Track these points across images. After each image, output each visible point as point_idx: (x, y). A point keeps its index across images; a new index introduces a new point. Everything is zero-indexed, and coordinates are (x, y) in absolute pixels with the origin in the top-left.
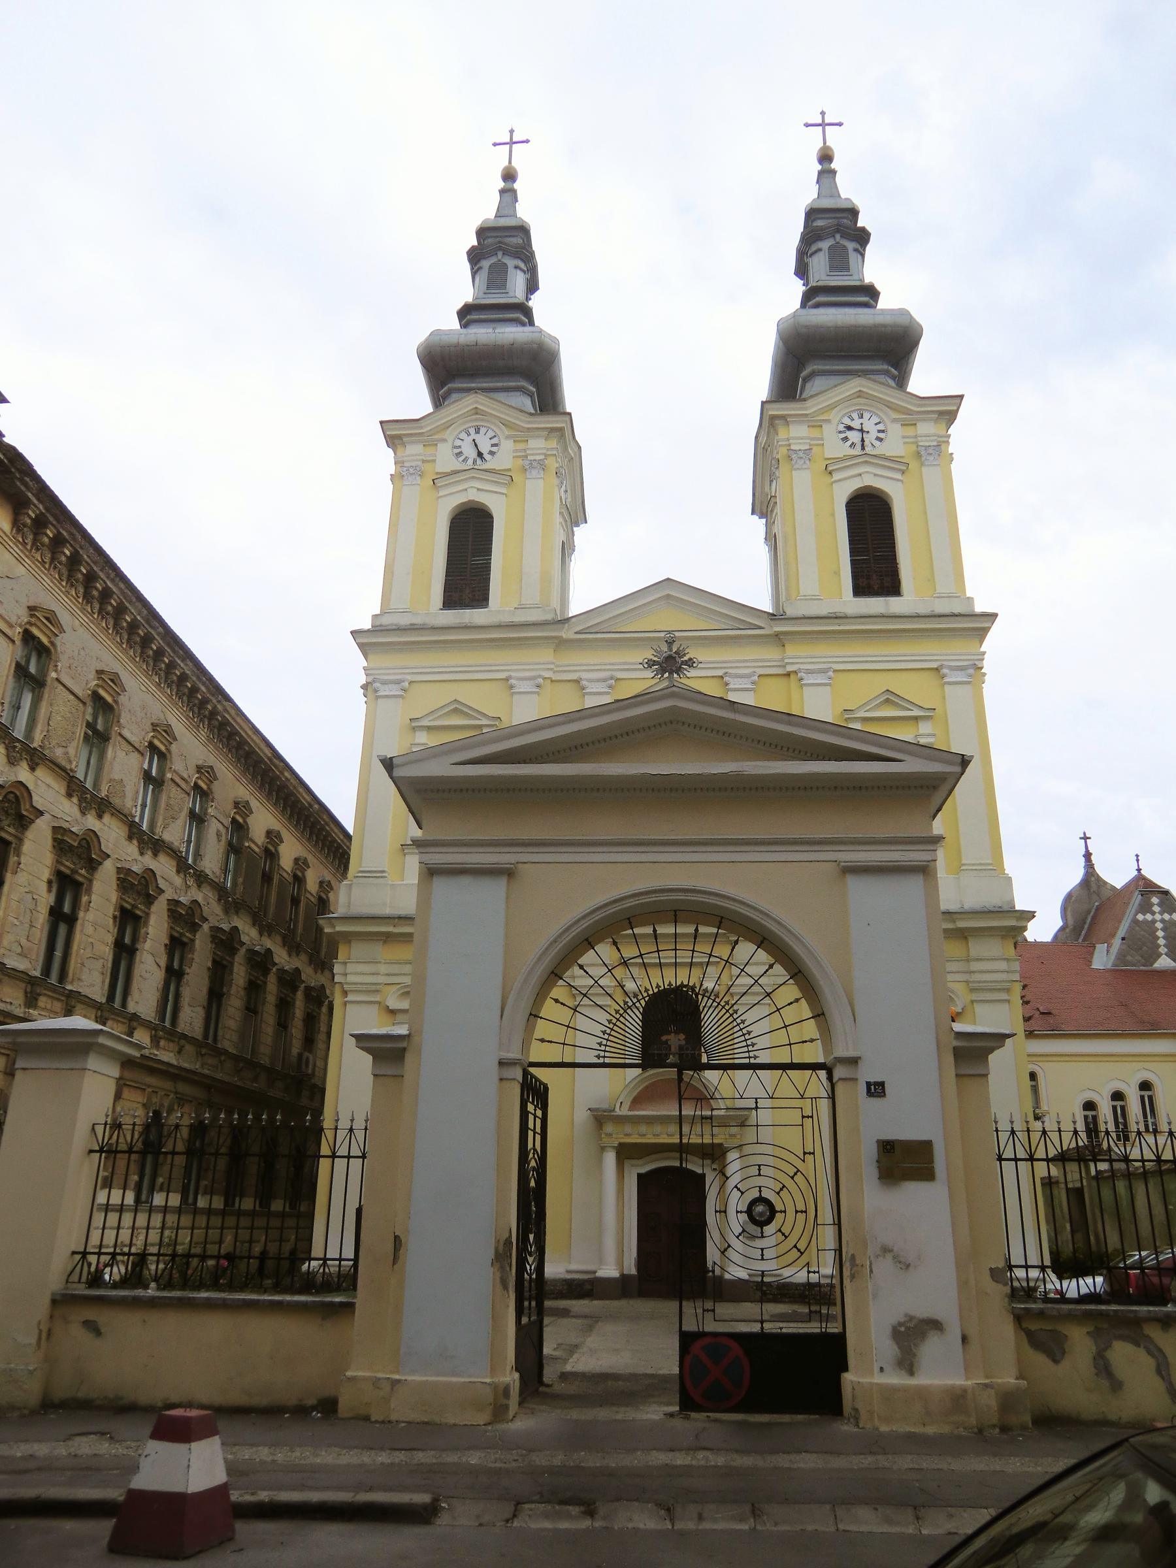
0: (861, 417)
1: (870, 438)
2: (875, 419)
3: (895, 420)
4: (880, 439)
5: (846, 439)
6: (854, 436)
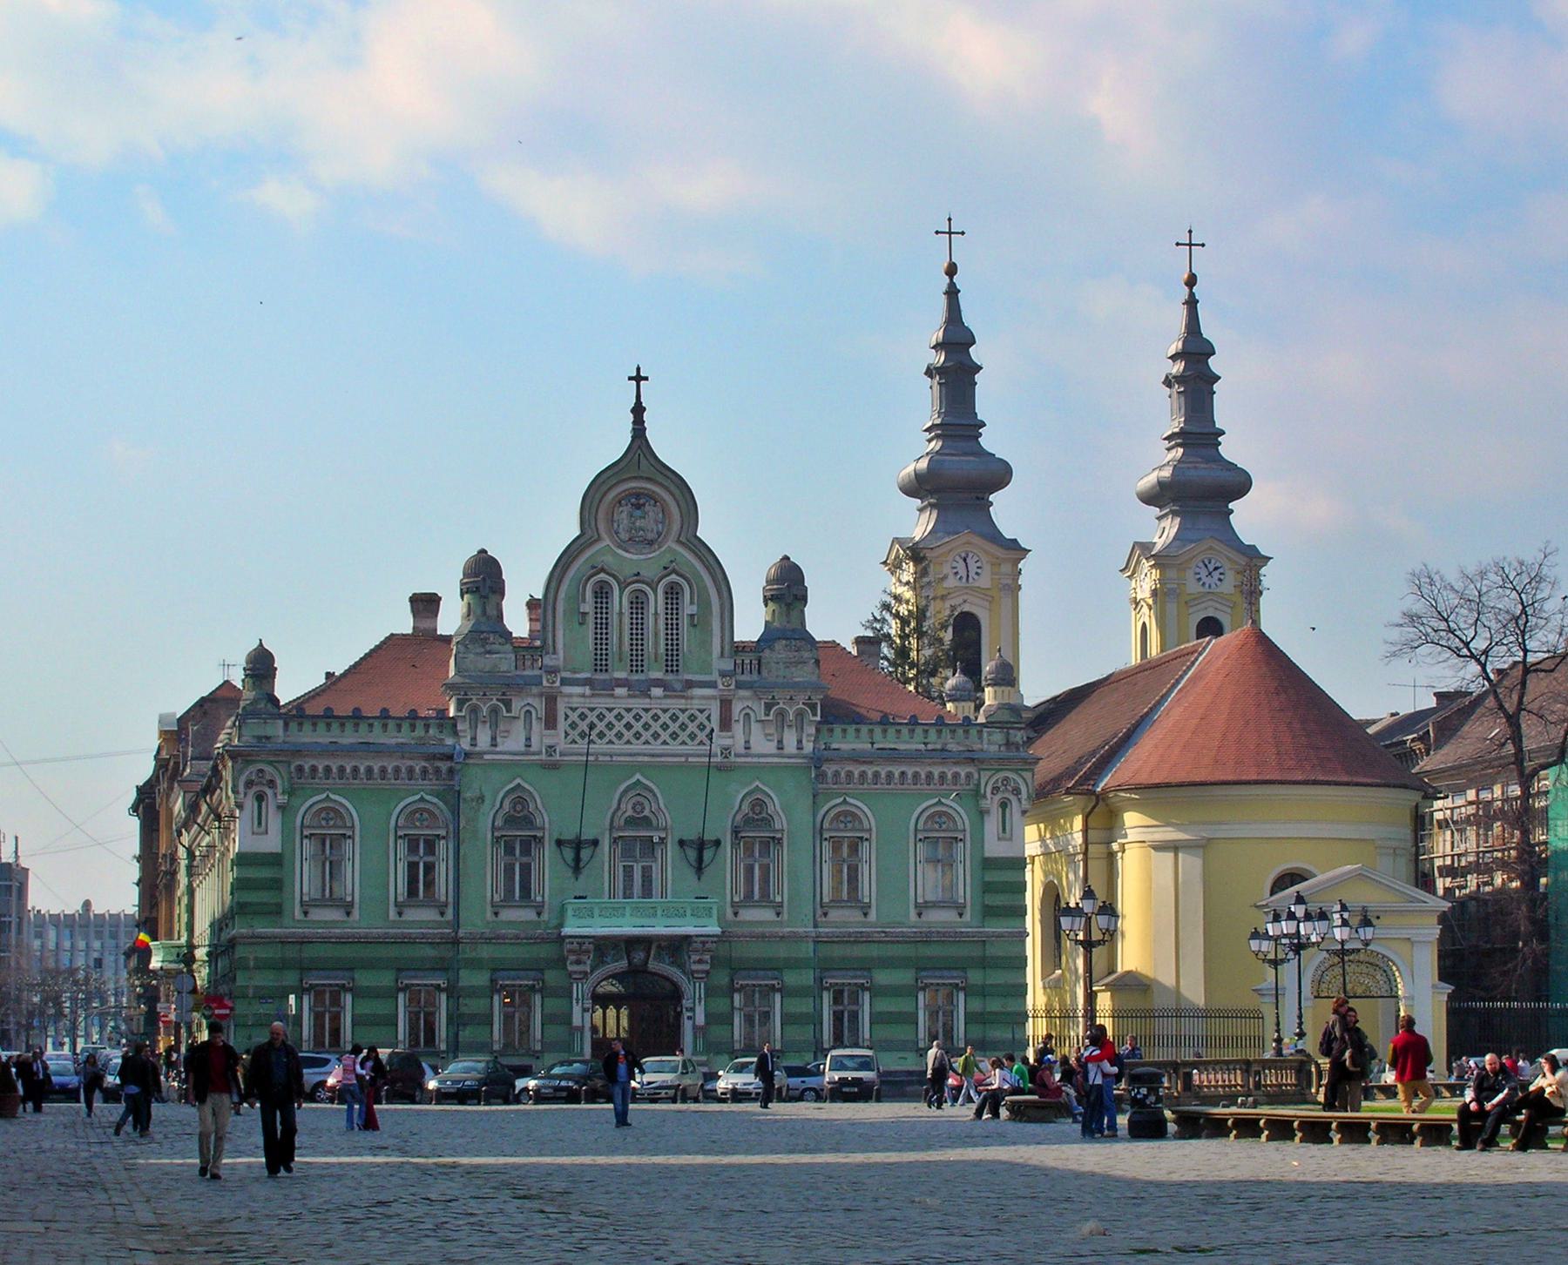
2: (976, 559)
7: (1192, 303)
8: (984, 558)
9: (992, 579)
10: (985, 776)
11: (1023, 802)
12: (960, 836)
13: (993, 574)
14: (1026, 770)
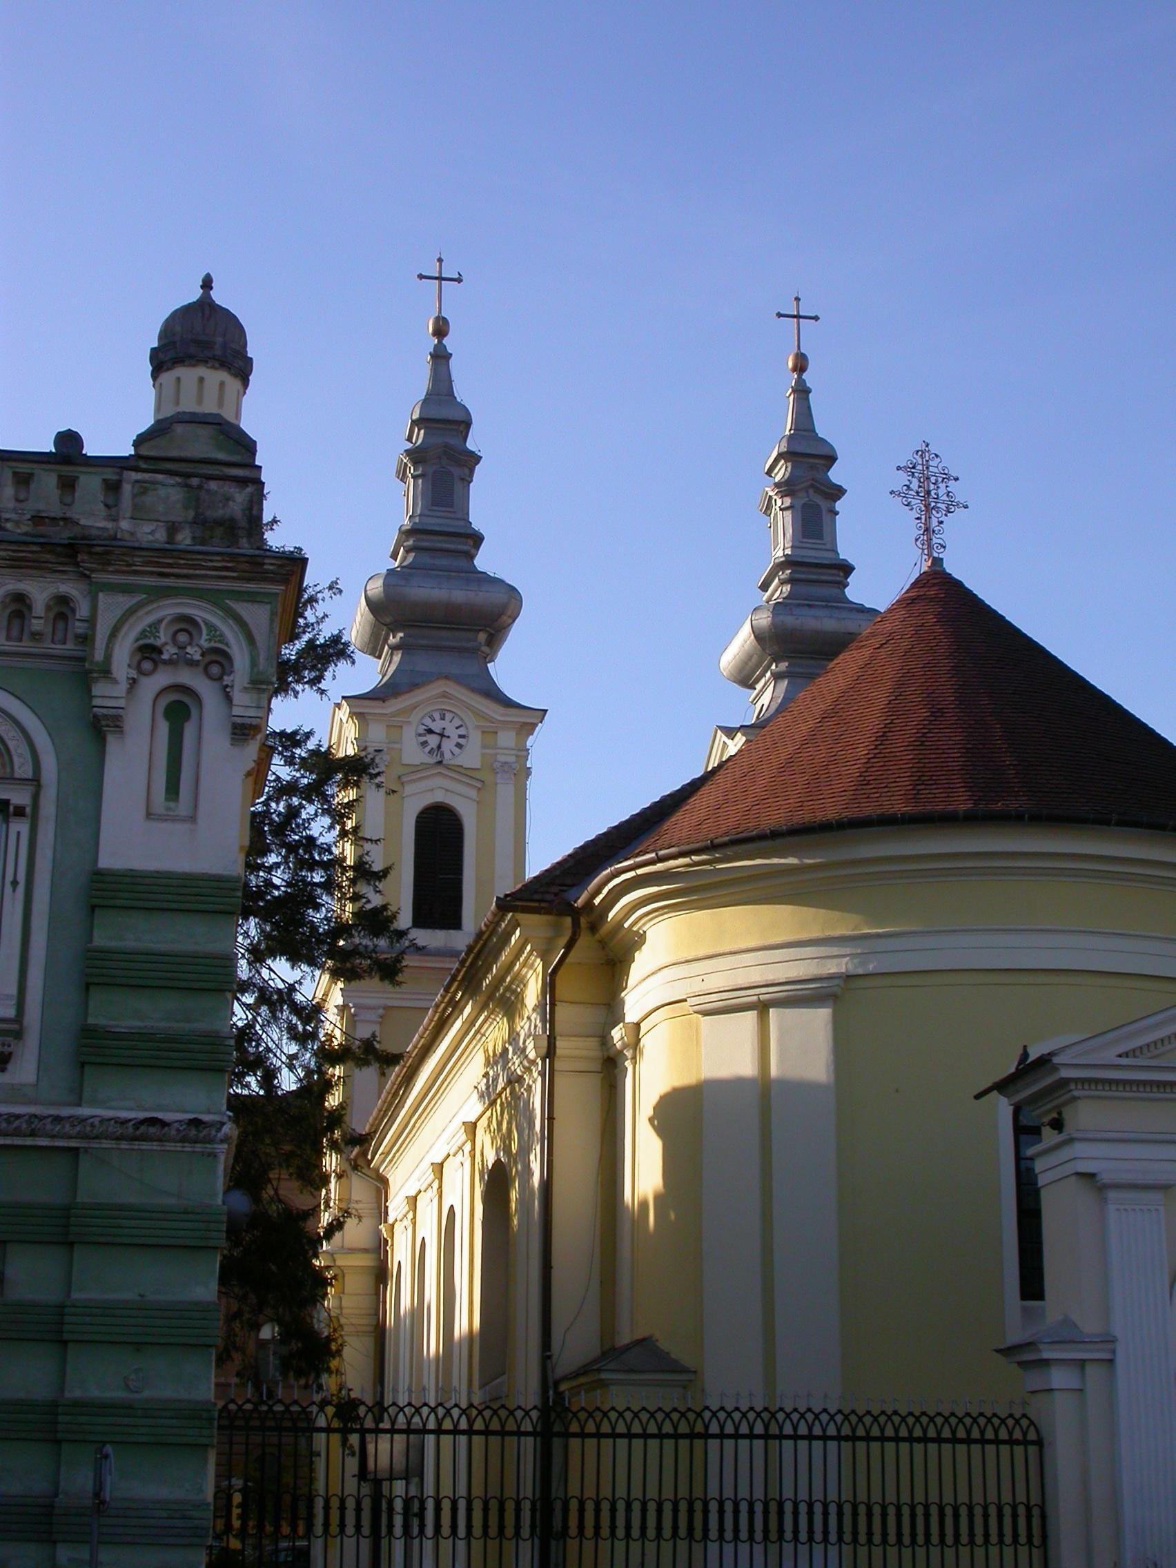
0: (443, 719)
1: (448, 746)
2: (457, 722)
3: (477, 727)
4: (459, 746)
5: (425, 744)
6: (433, 740)
7: (802, 392)
9: (483, 755)
10: (110, 607)
11: (238, 697)
12: (19, 797)
13: (484, 746)
14: (252, 598)
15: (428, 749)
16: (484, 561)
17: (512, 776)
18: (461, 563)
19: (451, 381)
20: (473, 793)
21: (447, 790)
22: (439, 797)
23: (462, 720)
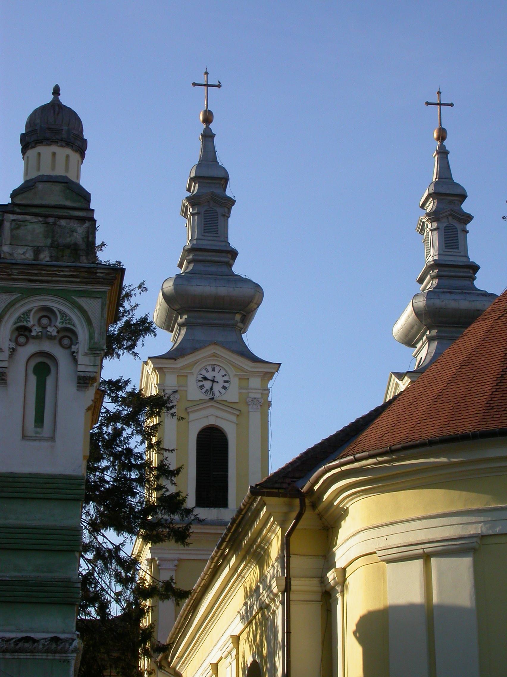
0: (214, 370)
1: (217, 388)
2: (223, 372)
3: (235, 375)
4: (224, 388)
5: (202, 387)
6: (207, 385)
7: (443, 153)
8: (232, 372)
9: (240, 393)
11: (81, 359)
13: (240, 388)
14: (89, 295)
15: (204, 390)
16: (238, 268)
17: (259, 407)
18: (224, 269)
19: (215, 152)
20: (234, 419)
21: (217, 417)
22: (212, 421)
23: (226, 371)
